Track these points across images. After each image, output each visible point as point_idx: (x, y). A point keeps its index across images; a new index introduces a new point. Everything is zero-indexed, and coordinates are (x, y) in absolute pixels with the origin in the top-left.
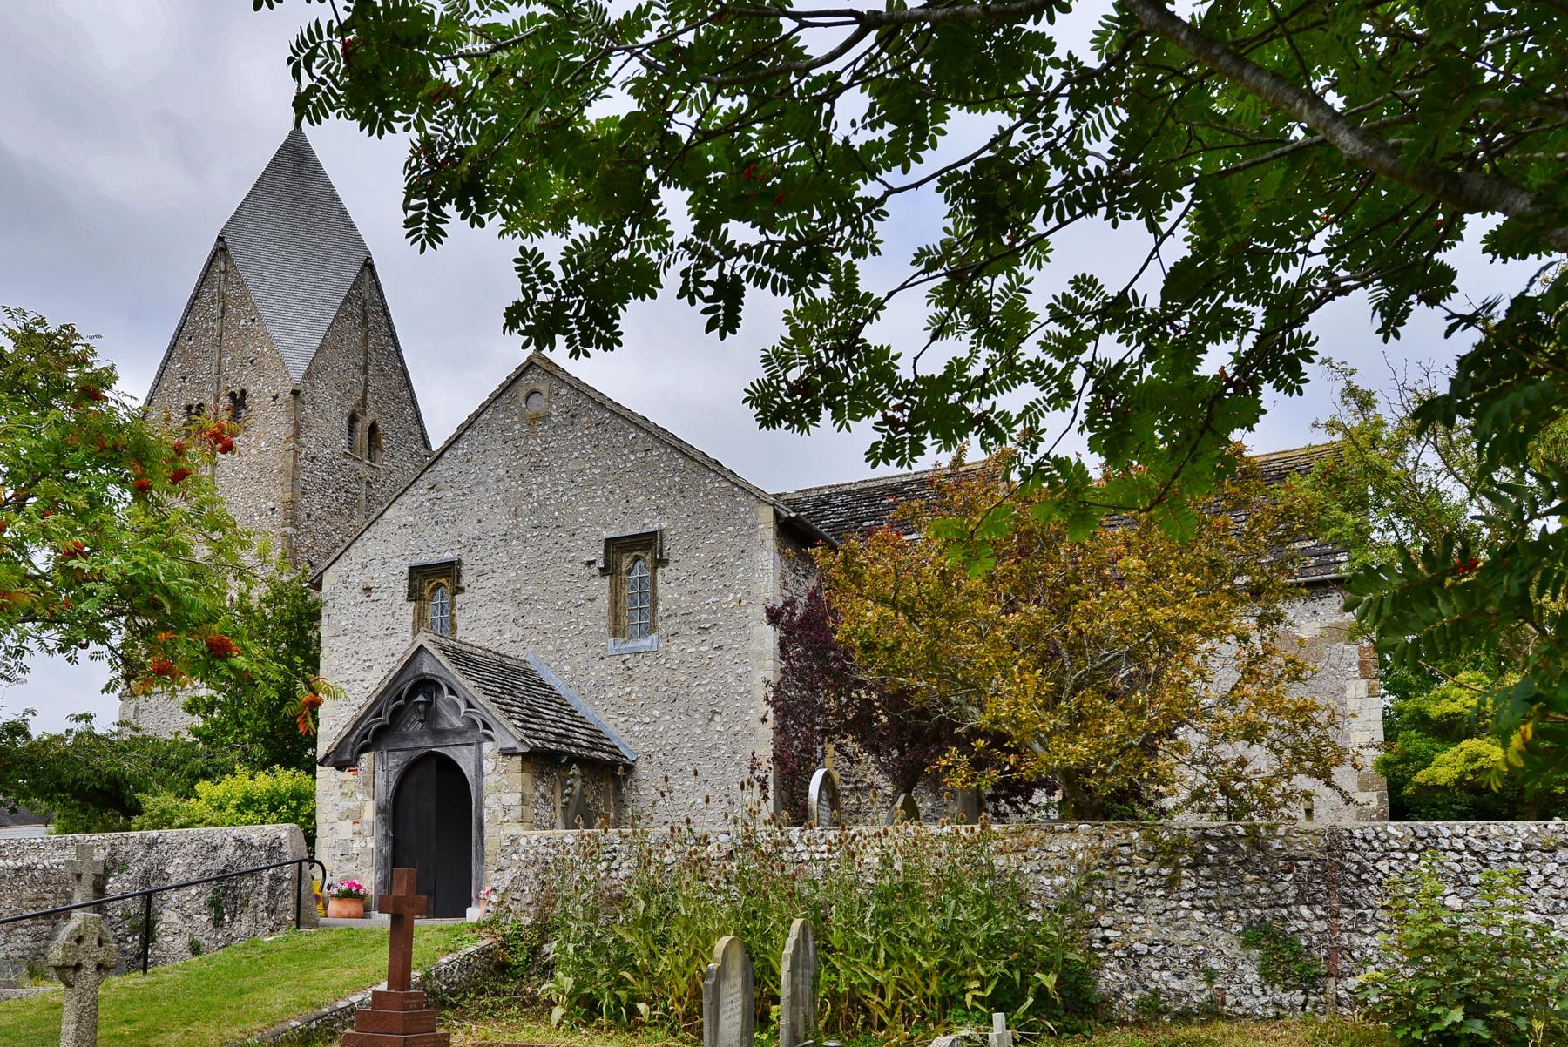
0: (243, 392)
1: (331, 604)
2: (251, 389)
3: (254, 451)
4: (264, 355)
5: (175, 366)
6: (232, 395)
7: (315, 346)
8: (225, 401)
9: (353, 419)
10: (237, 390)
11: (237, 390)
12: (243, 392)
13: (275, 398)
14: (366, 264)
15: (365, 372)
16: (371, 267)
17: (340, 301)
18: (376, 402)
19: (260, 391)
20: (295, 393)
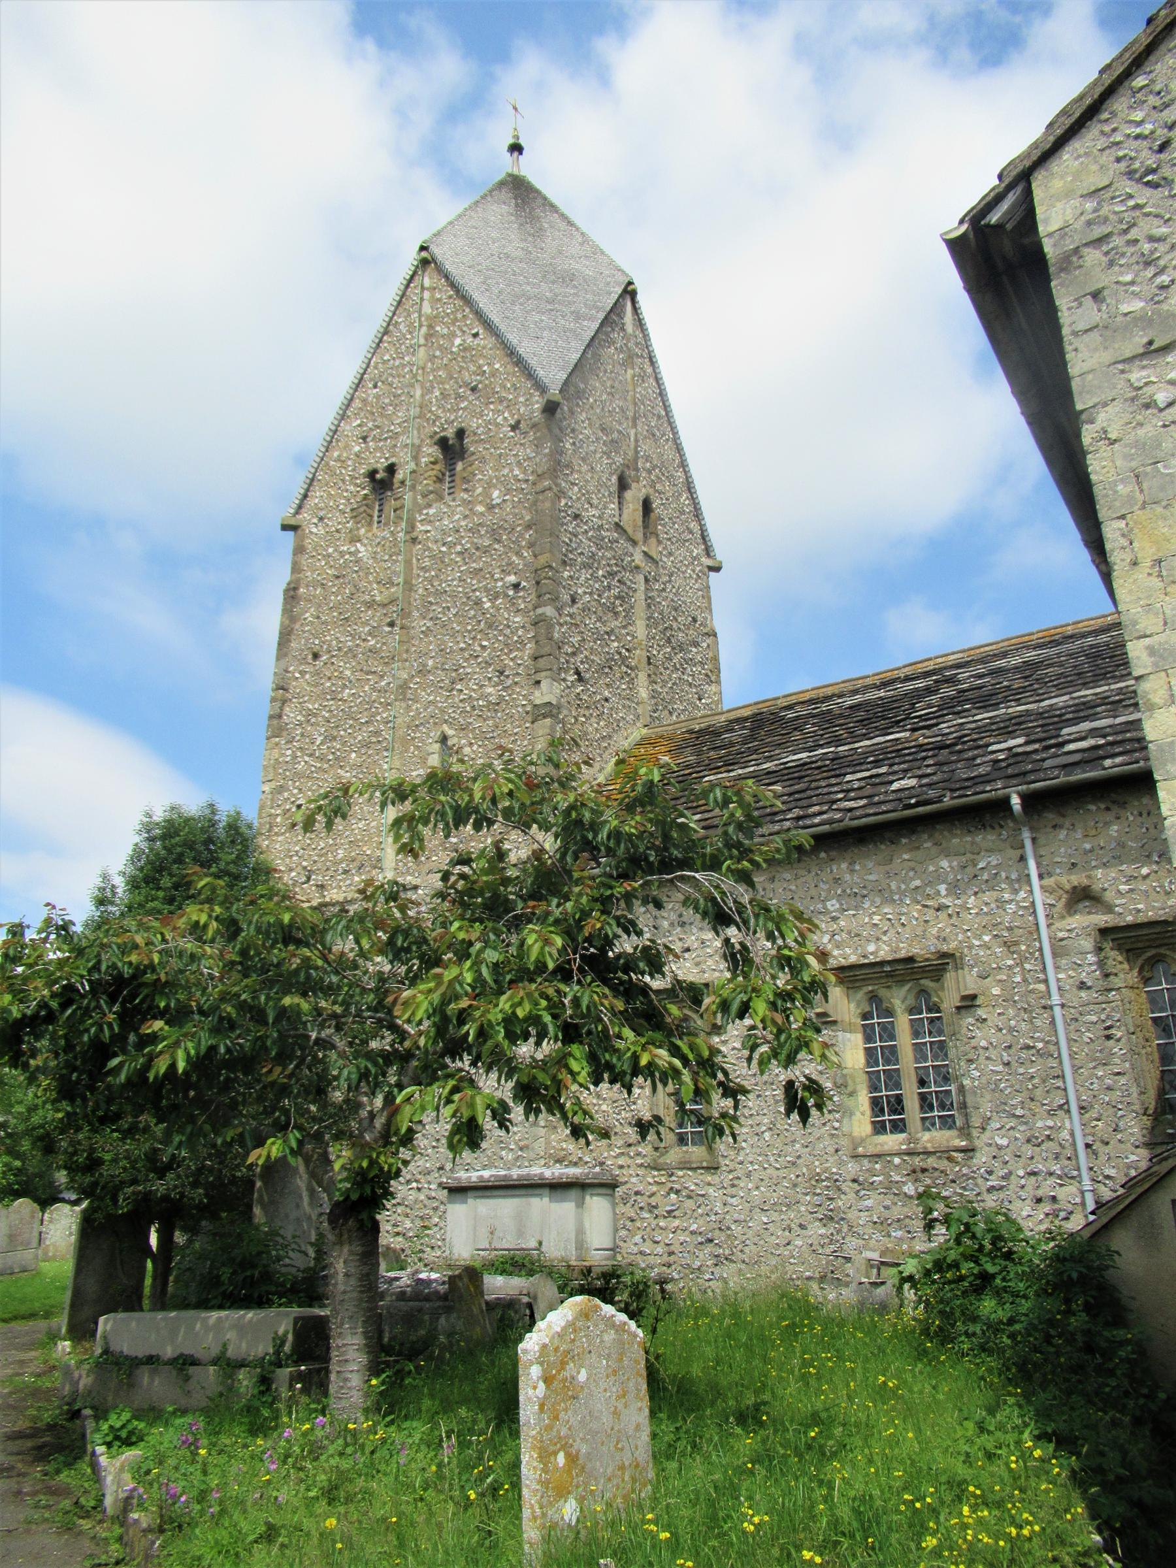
0: (461, 433)
1: (1093, 256)
2: (474, 424)
3: (480, 509)
4: (494, 374)
5: (350, 428)
6: (443, 443)
7: (576, 356)
8: (431, 452)
9: (623, 485)
10: (450, 433)
11: (450, 433)
12: (461, 433)
13: (514, 428)
14: (625, 291)
15: (635, 426)
16: (633, 294)
17: (601, 315)
18: (649, 472)
19: (486, 421)
20: (551, 409)
